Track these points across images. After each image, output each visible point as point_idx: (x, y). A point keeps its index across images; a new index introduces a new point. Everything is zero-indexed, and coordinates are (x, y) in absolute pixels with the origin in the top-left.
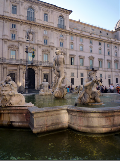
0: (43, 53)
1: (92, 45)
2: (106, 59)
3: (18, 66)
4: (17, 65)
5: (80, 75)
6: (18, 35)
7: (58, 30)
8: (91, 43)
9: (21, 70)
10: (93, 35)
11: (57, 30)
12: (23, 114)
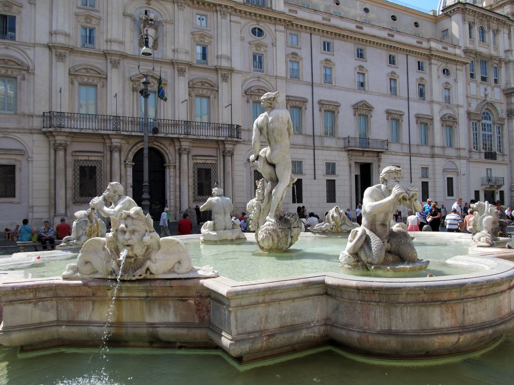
0: (193, 94)
2: (413, 113)
3: (107, 141)
4: (102, 135)
5: (324, 168)
6: (102, 33)
7: (245, 12)
8: (360, 55)
9: (116, 155)
10: (366, 30)
11: (240, 11)
12: (186, 300)
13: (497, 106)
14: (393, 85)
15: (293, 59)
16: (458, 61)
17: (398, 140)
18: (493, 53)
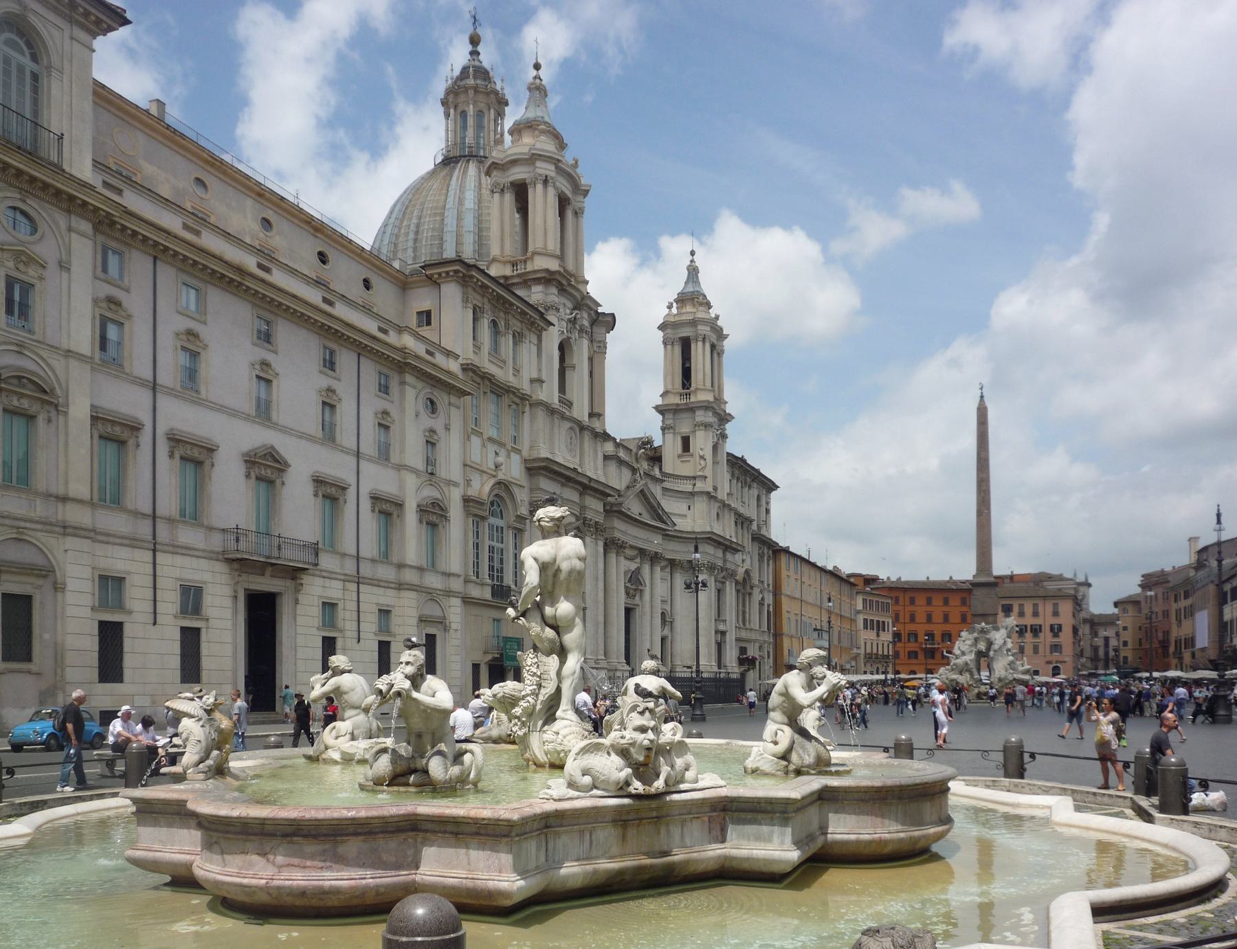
1: (270, 357)
13: (516, 490)
14: (327, 418)
15: (109, 315)
16: (454, 386)
17: (333, 549)
18: (511, 380)
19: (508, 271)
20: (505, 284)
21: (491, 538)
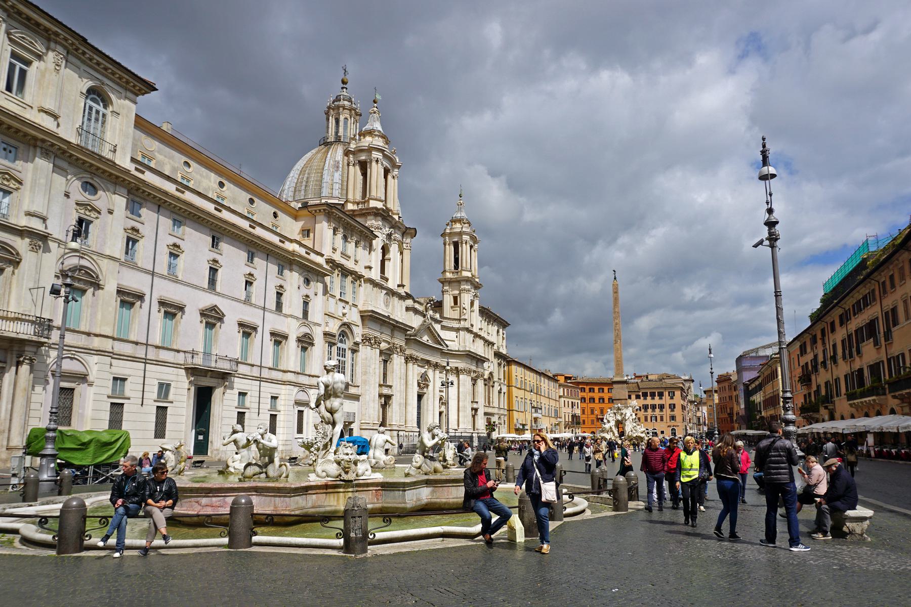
1: (218, 257)
10: (225, 215)
13: (354, 328)
19: (355, 207)
20: (353, 215)
21: (339, 355)
